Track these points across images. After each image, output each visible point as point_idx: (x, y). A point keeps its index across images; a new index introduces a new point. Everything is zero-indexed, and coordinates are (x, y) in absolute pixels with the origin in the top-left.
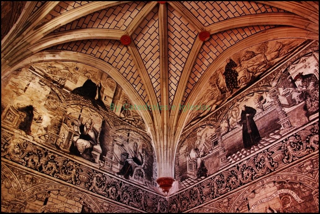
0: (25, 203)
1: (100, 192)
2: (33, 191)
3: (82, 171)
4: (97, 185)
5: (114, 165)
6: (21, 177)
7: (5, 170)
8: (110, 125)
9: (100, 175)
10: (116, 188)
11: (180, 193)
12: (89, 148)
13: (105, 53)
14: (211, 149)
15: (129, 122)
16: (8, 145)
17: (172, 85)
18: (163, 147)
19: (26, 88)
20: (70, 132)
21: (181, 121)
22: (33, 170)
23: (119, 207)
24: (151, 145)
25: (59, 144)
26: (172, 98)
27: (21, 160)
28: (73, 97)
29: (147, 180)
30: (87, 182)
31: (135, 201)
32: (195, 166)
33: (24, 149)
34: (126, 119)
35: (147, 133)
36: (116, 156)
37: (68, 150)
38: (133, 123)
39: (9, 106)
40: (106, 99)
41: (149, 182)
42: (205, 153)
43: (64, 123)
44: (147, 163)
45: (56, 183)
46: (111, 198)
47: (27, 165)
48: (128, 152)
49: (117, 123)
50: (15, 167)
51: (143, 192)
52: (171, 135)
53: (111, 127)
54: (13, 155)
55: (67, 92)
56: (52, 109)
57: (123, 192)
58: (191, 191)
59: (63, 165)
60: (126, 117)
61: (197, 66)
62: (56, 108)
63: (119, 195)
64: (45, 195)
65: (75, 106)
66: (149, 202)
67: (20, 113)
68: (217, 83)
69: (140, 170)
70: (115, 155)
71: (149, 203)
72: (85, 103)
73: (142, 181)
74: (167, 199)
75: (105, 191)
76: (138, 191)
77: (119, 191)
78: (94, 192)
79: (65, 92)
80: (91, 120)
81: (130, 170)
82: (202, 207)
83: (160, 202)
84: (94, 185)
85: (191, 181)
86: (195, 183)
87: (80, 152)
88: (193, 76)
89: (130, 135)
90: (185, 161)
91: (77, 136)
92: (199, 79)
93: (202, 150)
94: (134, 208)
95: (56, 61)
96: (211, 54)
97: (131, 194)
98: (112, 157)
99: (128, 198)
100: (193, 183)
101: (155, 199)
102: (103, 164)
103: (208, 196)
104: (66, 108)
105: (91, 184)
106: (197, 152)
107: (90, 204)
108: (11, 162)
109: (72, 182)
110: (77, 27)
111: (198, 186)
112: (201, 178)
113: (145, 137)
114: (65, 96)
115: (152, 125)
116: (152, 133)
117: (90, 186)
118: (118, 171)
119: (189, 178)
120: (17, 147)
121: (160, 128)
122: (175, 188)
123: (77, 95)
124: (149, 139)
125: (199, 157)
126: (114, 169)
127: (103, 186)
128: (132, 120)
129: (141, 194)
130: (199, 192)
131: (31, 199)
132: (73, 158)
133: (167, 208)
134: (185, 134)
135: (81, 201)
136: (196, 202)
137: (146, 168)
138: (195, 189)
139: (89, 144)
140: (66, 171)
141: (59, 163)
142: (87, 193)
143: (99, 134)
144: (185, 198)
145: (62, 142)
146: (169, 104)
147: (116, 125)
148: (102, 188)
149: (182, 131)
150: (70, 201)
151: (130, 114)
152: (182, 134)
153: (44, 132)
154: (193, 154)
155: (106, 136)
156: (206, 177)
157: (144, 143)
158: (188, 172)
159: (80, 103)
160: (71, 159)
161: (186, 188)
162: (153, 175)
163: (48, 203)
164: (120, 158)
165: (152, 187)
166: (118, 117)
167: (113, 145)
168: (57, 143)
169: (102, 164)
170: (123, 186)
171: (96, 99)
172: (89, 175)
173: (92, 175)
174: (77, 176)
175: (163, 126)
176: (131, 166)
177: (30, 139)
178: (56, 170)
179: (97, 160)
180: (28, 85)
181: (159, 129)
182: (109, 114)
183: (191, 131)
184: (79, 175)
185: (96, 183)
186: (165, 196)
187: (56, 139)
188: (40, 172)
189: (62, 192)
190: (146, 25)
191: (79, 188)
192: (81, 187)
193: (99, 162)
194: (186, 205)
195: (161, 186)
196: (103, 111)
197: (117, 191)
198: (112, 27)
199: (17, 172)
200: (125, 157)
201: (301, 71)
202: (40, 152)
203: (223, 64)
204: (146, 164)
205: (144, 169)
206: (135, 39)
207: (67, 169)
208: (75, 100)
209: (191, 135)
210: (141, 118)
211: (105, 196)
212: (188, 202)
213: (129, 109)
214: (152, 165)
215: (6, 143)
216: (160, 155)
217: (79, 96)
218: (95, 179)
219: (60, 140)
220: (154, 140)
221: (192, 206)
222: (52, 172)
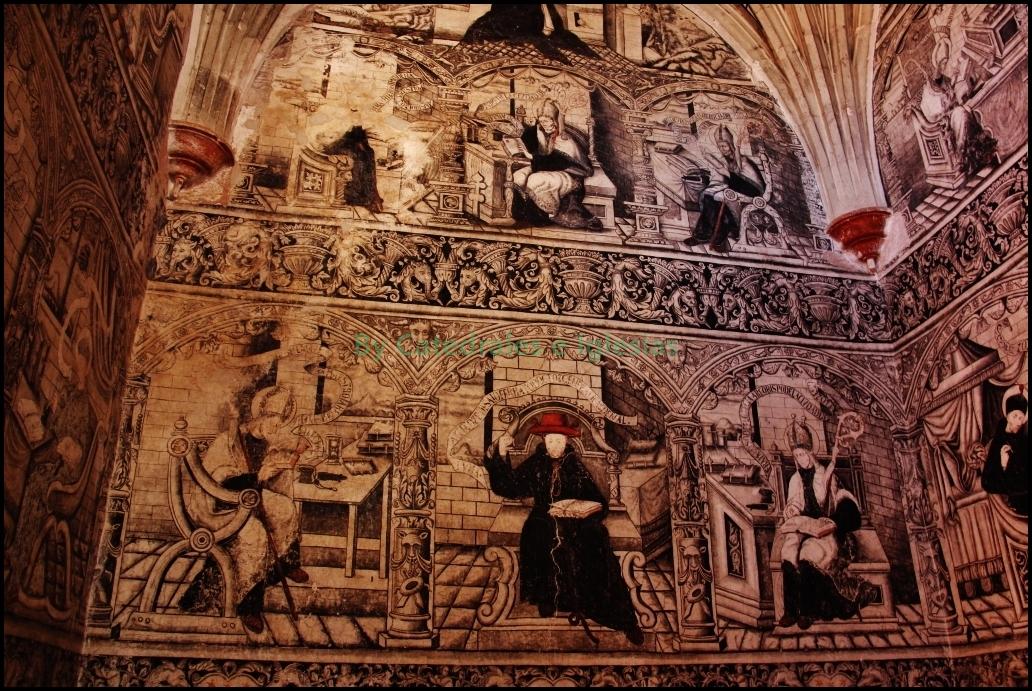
0: (434, 400)
1: (646, 313)
2: (444, 363)
3: (571, 267)
4: (630, 295)
5: (666, 221)
6: (399, 333)
7: (350, 327)
8: (618, 99)
9: (629, 264)
10: (693, 289)
11: (919, 250)
12: (572, 192)
14: (996, 59)
15: (680, 69)
16: (334, 258)
18: (824, 114)
19: (325, 83)
20: (497, 165)
22: (424, 308)
23: (718, 345)
24: (779, 119)
25: (475, 211)
27: (382, 289)
28: (471, 55)
29: (793, 239)
30: (596, 294)
31: (768, 315)
32: (947, 142)
33: (381, 257)
34: (669, 63)
35: (753, 83)
36: (667, 188)
37: (508, 219)
38: (696, 67)
39: (296, 154)
40: (580, 22)
41: (803, 241)
42: (972, 82)
43: (470, 141)
44: (778, 182)
45: (501, 323)
46: (687, 325)
47: (403, 298)
48: (704, 167)
49: (641, 85)
50: (375, 313)
51: (789, 277)
52: (840, 63)
53: (624, 105)
54: (358, 283)
55: (450, 47)
56: (420, 113)
57: (721, 296)
58: (951, 234)
59: (508, 265)
60: (668, 56)
62: (432, 108)
63: (711, 309)
64: (482, 365)
65: (487, 78)
66: (816, 307)
67: (334, 159)
69: (760, 212)
70: (663, 189)
71: (819, 308)
72: (517, 57)
73: (776, 244)
74: (878, 283)
75: (660, 307)
76: (769, 281)
77: (706, 297)
78: (626, 320)
79: (443, 49)
80: (553, 104)
81: (727, 221)
82: (1002, 274)
83: (856, 297)
84: (620, 297)
85: (945, 197)
86: (961, 201)
87: (547, 214)
89: (697, 108)
90: (908, 137)
91: (522, 166)
93: (961, 78)
94: (768, 337)
97: (747, 296)
98: (655, 198)
99: (743, 311)
100: (953, 204)
101: (834, 291)
102: (631, 228)
103: (1017, 231)
104: (461, 97)
105: (610, 297)
106: (944, 91)
107: (624, 360)
108: (357, 303)
109: (549, 307)
111: (973, 208)
112: (979, 177)
113: (752, 98)
114: (446, 62)
115: (764, 51)
116: (771, 79)
117: (607, 305)
118: (688, 235)
119: (936, 191)
120: (359, 258)
121: (794, 52)
122: (896, 239)
123: (481, 43)
124: (766, 101)
125: (957, 104)
126: (670, 233)
127: (649, 295)
128: (691, 59)
129: (784, 286)
130: (980, 227)
131: (446, 386)
132: (530, 237)
133: (885, 312)
134: (887, 42)
135: (592, 355)
136: (978, 264)
137: (780, 198)
138: (965, 221)
139: (569, 177)
140: (522, 280)
141: (494, 265)
142: (603, 327)
143: (591, 139)
144: (938, 262)
145: (482, 199)
147: (640, 93)
148: (649, 300)
149: (875, 34)
150: (557, 366)
151: (677, 42)
152: (878, 45)
153: (420, 189)
154: (932, 103)
155: (617, 139)
156: (996, 166)
157: (753, 121)
158: (929, 169)
159: (500, 64)
160: (524, 241)
161: (933, 228)
162: (812, 217)
163: (497, 386)
164: (681, 194)
165: (818, 256)
166: (638, 65)
167: (648, 159)
168: (468, 209)
169: (627, 230)
170: (714, 276)
171: (547, 33)
172: (596, 271)
173: (606, 270)
174: (558, 286)
175: (803, 40)
176: (726, 207)
177: (387, 223)
178: (492, 288)
179: (609, 219)
180: (328, 70)
181: (790, 54)
182: (604, 65)
183: (907, 23)
184: (563, 283)
185: (625, 291)
186: (869, 275)
187: (461, 197)
188: (444, 306)
189: (527, 346)
191: (575, 320)
192: (582, 314)
193: (616, 224)
194: (947, 283)
195: (847, 245)
196: (583, 62)
197: (698, 297)
199: (383, 325)
200: (698, 185)
202: (428, 251)
204: (778, 186)
205: (774, 206)
207: (522, 275)
208: (481, 60)
209: (909, 36)
210: (720, 42)
211: (664, 323)
212: (950, 272)
213: (669, 26)
214: (799, 183)
215: (328, 256)
216: (817, 144)
217: (491, 45)
218: (617, 278)
219: (474, 197)
220: (783, 99)
221: (966, 283)
222: (481, 295)
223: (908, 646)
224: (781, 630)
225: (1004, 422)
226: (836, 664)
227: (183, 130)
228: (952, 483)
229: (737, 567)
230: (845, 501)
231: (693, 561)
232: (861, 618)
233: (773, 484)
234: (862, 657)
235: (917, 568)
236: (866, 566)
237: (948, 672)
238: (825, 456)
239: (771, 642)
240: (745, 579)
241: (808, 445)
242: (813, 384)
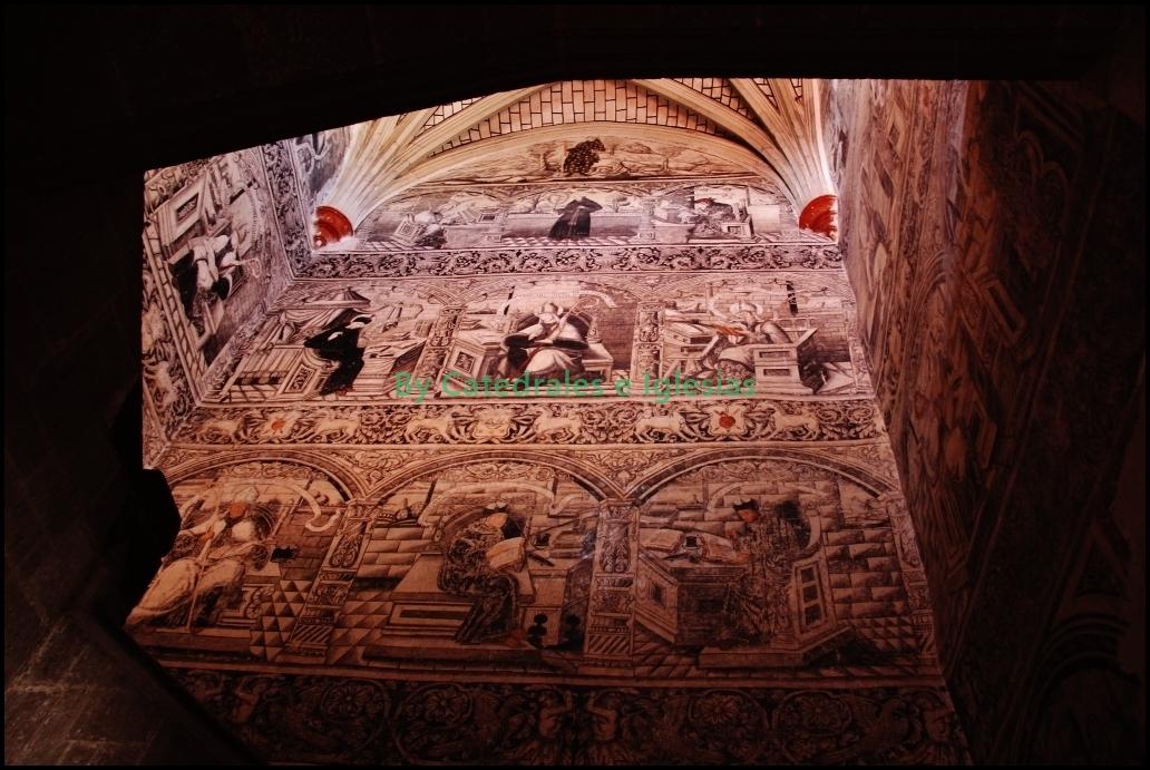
21: (424, 168)
29: (308, 184)
61: (525, 107)
68: (545, 155)
88: (505, 117)
90: (396, 220)
96: (568, 108)
122: (346, 244)
149: (415, 184)
201: (713, 197)
203: (578, 138)
216: (350, 179)
223: (190, 370)
224: (167, 267)
225: (349, 324)
226: (166, 319)
228: (281, 337)
229: (182, 213)
230: (226, 281)
231: (172, 180)
232: (189, 326)
233: (220, 222)
234: (175, 338)
235: (219, 356)
236: (209, 315)
237: (190, 408)
238: (240, 255)
239: (159, 259)
240: (178, 225)
241: (241, 241)
242: (263, 230)
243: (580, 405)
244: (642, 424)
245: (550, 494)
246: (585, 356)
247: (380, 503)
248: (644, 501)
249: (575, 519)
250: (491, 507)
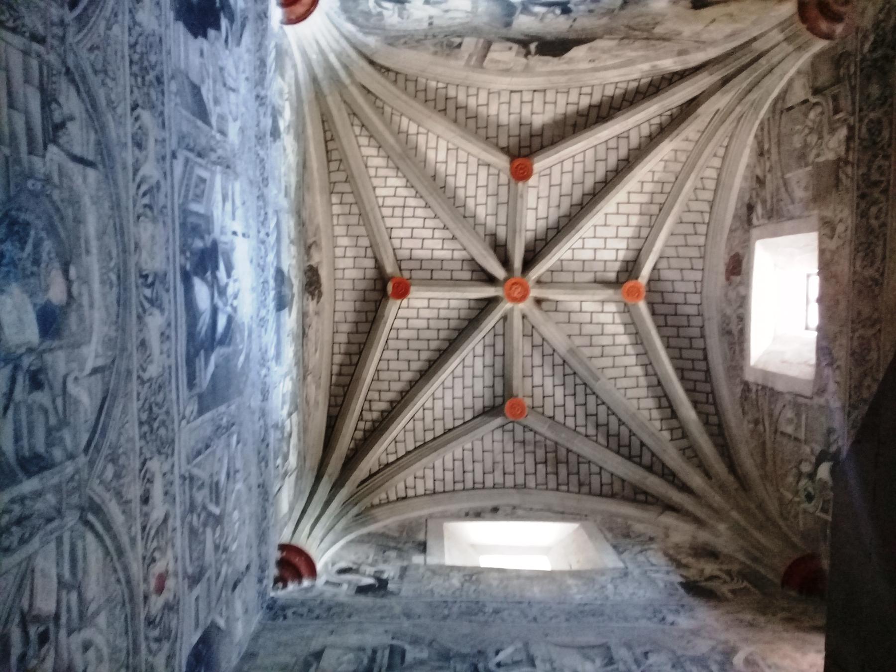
13: (538, 106)
17: (373, 151)
26: (357, 130)
61: (354, 220)
88: (349, 198)
92: (332, 204)
95: (647, 59)
110: (625, 135)
146: (354, 114)
190: (496, 214)
198: (556, 170)
206: (498, 175)
227: (828, 36)
243: (170, 367)
244: (154, 465)
245: (89, 366)
246: (206, 350)
247: (68, 71)
248: (87, 523)
249: (64, 423)
250: (73, 272)
